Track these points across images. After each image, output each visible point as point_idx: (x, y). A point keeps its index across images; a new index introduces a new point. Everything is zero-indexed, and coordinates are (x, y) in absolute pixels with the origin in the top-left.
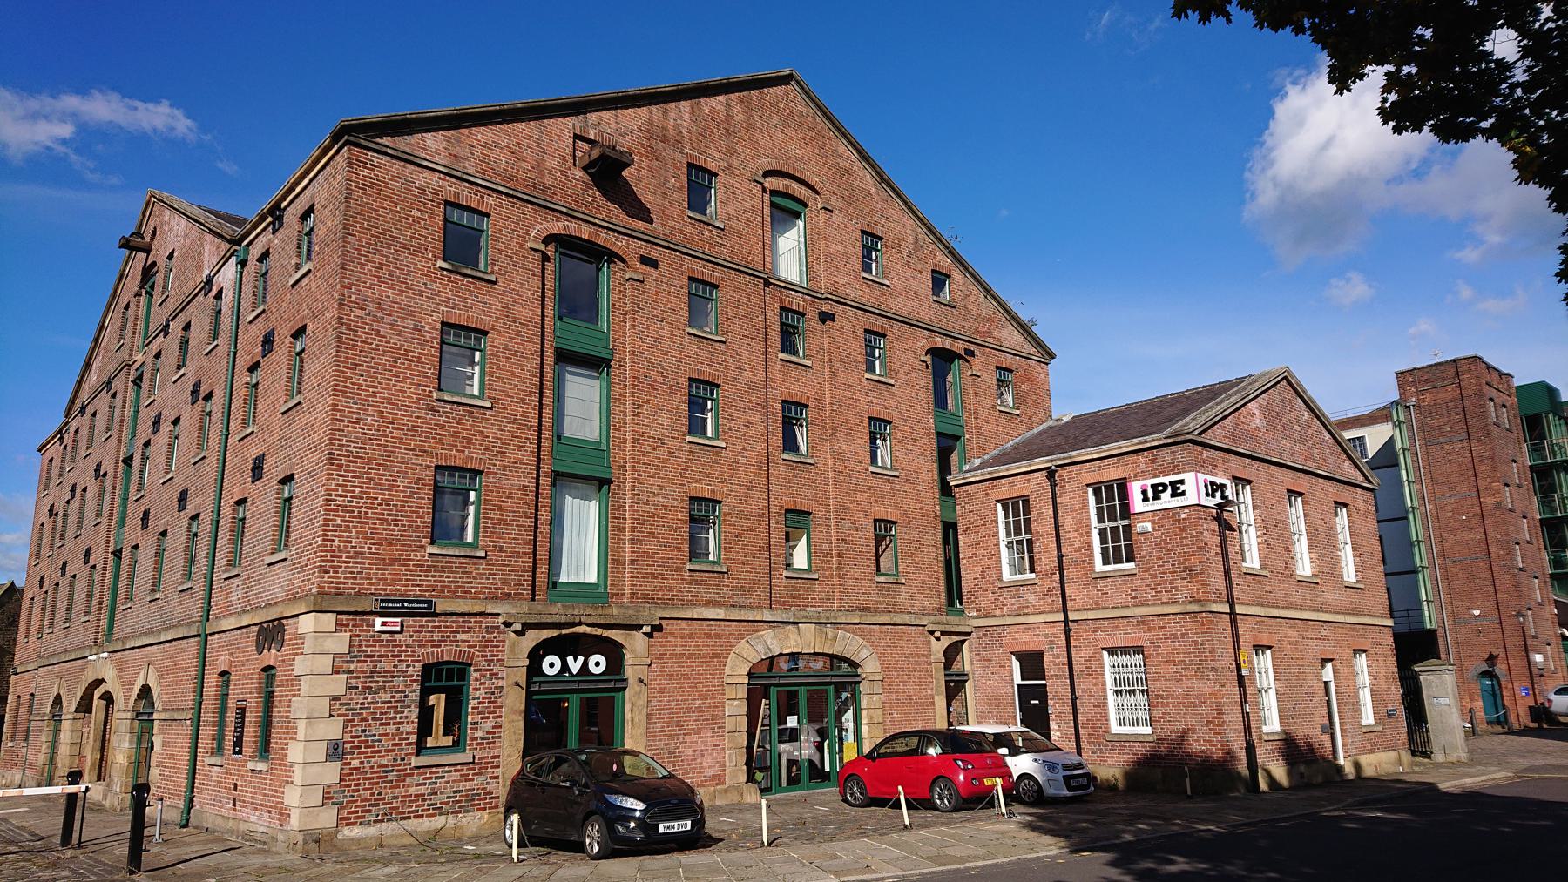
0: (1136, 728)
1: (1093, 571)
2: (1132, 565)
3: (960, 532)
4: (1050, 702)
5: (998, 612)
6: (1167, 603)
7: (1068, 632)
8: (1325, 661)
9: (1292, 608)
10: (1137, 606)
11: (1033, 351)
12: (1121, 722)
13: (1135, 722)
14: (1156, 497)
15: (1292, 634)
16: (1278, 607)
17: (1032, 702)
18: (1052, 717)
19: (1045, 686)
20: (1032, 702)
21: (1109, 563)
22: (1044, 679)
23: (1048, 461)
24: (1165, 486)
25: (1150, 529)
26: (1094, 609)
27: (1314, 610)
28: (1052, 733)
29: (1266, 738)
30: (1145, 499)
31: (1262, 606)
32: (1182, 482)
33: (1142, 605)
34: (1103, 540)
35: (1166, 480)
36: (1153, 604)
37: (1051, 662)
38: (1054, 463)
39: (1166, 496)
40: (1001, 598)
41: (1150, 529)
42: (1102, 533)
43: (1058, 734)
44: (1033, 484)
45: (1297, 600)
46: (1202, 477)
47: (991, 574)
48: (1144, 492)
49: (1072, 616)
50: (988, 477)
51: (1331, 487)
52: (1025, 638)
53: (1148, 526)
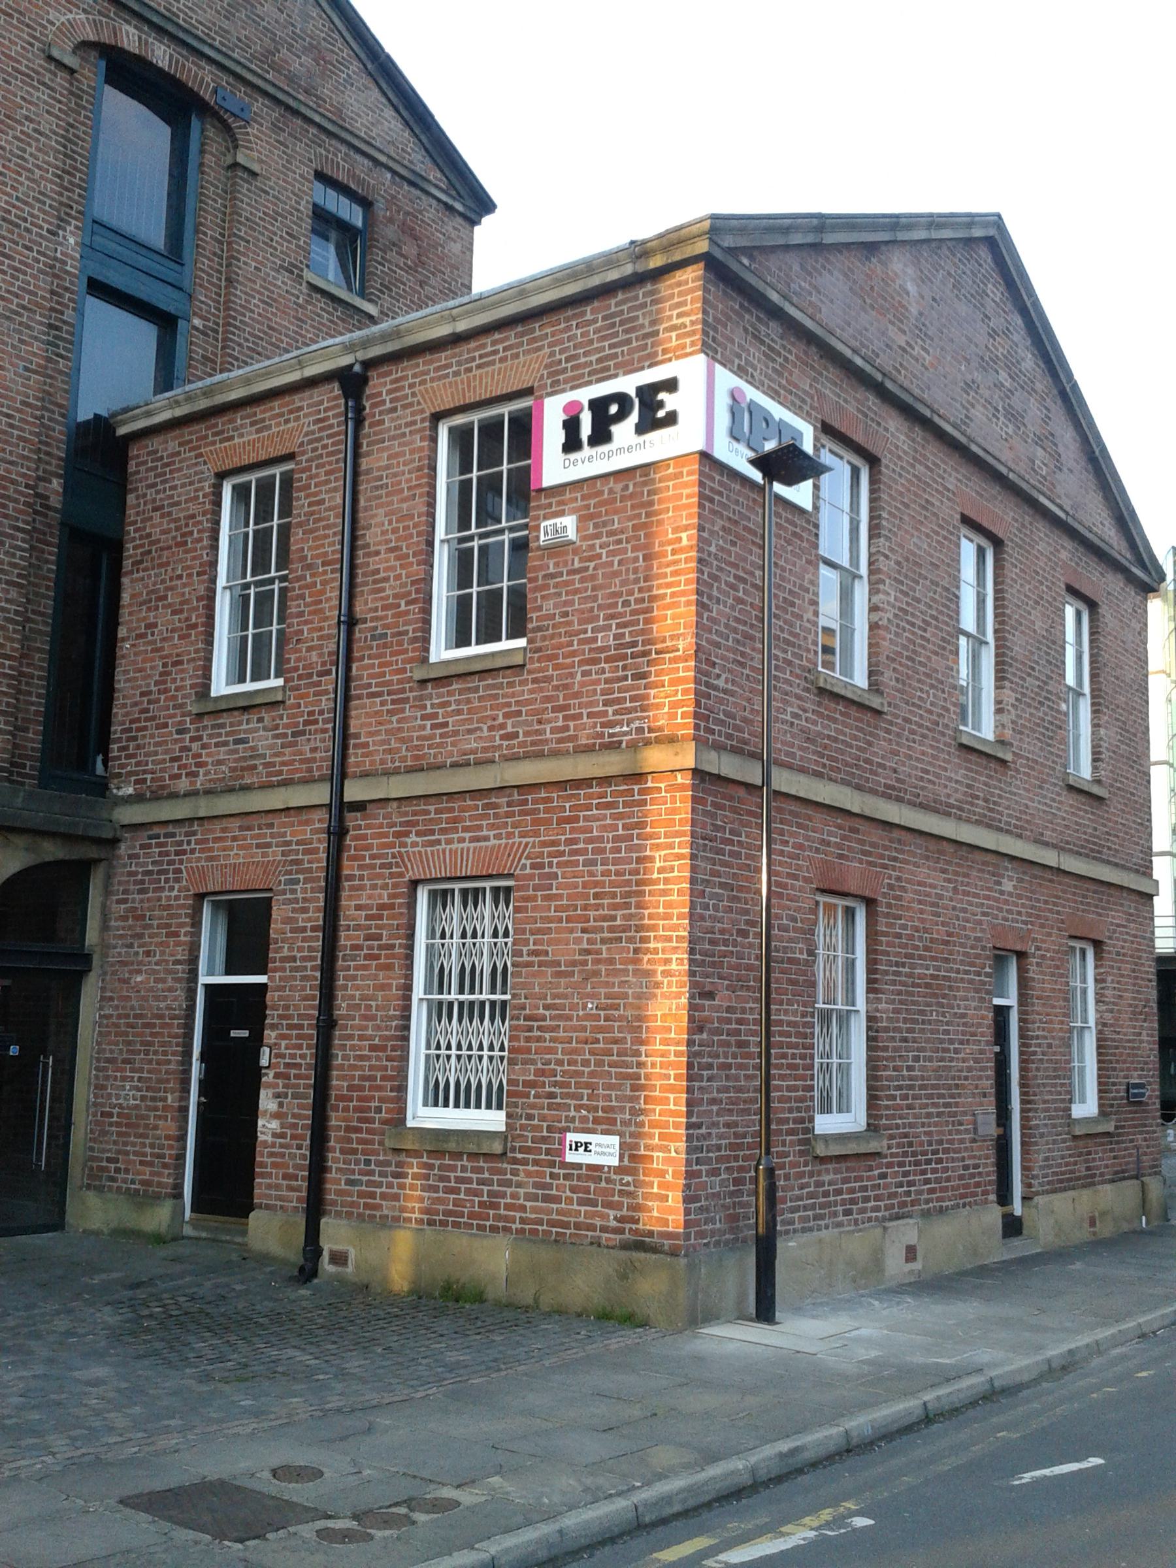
0: (472, 1113)
1: (425, 660)
2: (521, 642)
3: (127, 564)
4: (270, 1035)
5: (183, 785)
6: (589, 749)
7: (337, 835)
8: (1000, 959)
9: (937, 811)
10: (515, 758)
11: (434, 175)
12: (437, 1096)
13: (467, 1097)
14: (601, 436)
15: (926, 873)
16: (899, 800)
17: (234, 1034)
18: (268, 1077)
19: (263, 987)
20: (234, 1034)
21: (467, 643)
22: (263, 971)
23: (350, 348)
24: (622, 399)
25: (572, 534)
26: (410, 770)
27: (989, 826)
28: (260, 1122)
29: (821, 1150)
30: (572, 444)
31: (858, 787)
32: (671, 385)
33: (527, 756)
34: (463, 577)
35: (627, 384)
36: (555, 754)
37: (287, 920)
38: (362, 355)
39: (624, 431)
40: (195, 746)
41: (572, 534)
42: (463, 561)
43: (274, 1125)
44: (307, 422)
45: (953, 793)
46: (726, 379)
47: (188, 679)
48: (571, 426)
49: (354, 792)
50: (203, 404)
51: (1066, 551)
52: (236, 856)
53: (568, 525)
